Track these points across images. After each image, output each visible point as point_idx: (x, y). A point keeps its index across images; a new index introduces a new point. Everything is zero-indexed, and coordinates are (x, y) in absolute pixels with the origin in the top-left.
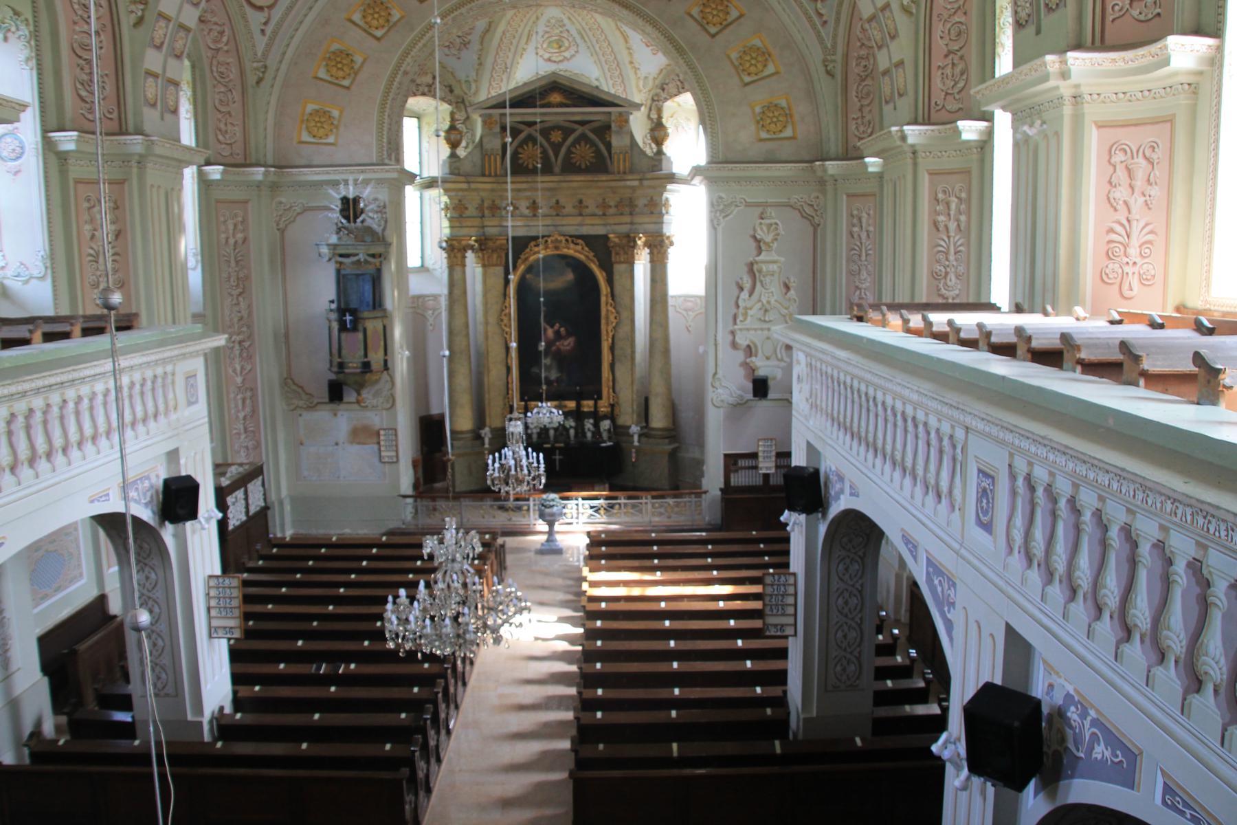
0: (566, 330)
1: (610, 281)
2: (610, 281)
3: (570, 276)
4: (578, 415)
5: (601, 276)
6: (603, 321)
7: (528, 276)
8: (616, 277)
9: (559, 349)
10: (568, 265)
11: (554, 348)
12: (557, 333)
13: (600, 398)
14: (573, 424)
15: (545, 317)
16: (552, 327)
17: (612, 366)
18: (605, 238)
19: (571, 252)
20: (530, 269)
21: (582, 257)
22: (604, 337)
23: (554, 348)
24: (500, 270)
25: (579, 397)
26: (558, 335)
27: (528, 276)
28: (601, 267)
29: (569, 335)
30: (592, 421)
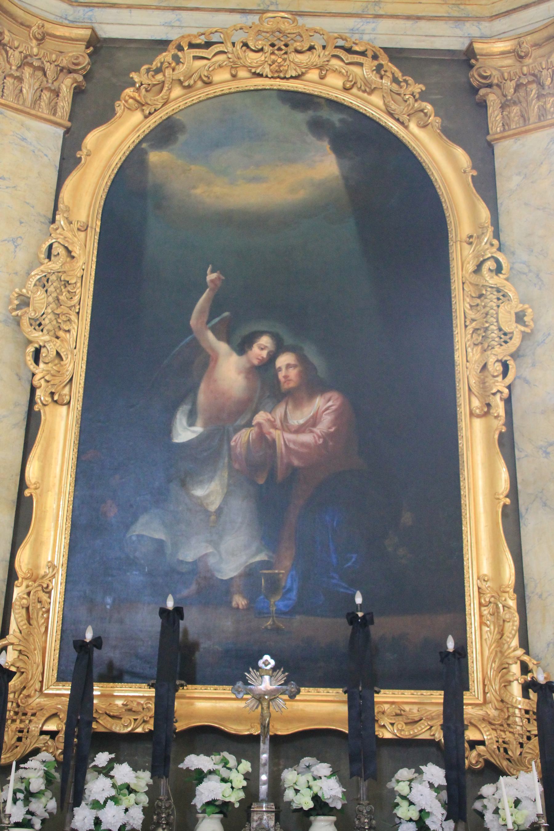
0: (302, 360)
1: (486, 183)
2: (486, 183)
3: (324, 166)
4: (362, 753)
5: (445, 164)
6: (462, 338)
7: (155, 157)
8: (507, 183)
9: (264, 441)
10: (318, 127)
11: (243, 438)
12: (265, 370)
13: (449, 673)
14: (332, 790)
15: (215, 309)
16: (242, 347)
17: (511, 519)
18: (467, 58)
19: (332, 87)
20: (165, 133)
21: (373, 106)
22: (466, 403)
23: (243, 438)
24: (49, 139)
25: (358, 669)
26: (265, 383)
27: (155, 157)
28: (451, 134)
29: (312, 385)
30: (435, 773)
